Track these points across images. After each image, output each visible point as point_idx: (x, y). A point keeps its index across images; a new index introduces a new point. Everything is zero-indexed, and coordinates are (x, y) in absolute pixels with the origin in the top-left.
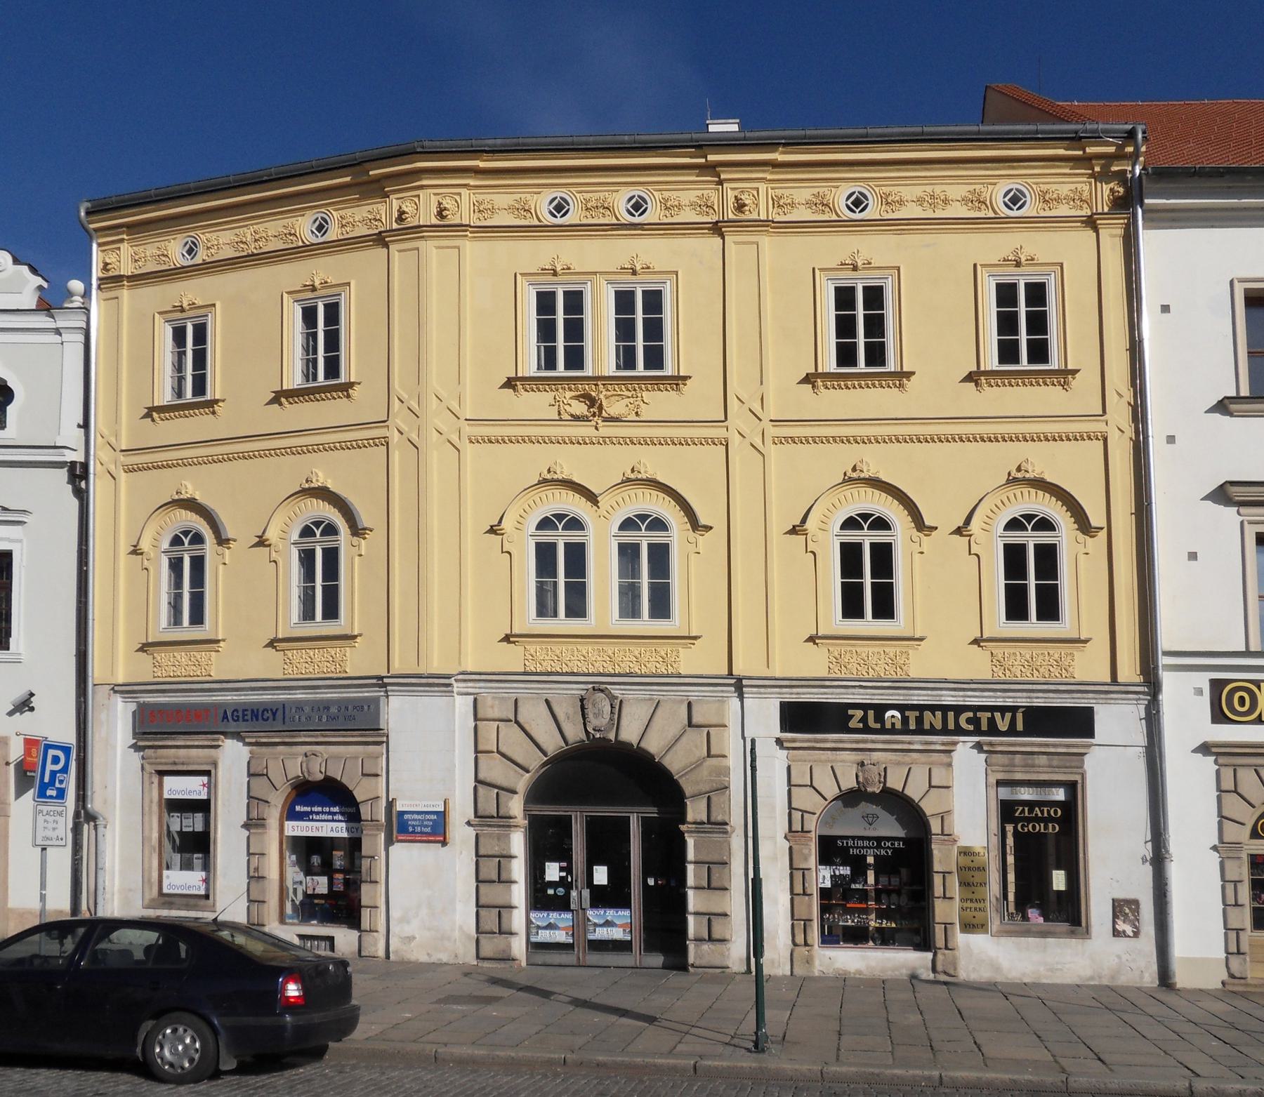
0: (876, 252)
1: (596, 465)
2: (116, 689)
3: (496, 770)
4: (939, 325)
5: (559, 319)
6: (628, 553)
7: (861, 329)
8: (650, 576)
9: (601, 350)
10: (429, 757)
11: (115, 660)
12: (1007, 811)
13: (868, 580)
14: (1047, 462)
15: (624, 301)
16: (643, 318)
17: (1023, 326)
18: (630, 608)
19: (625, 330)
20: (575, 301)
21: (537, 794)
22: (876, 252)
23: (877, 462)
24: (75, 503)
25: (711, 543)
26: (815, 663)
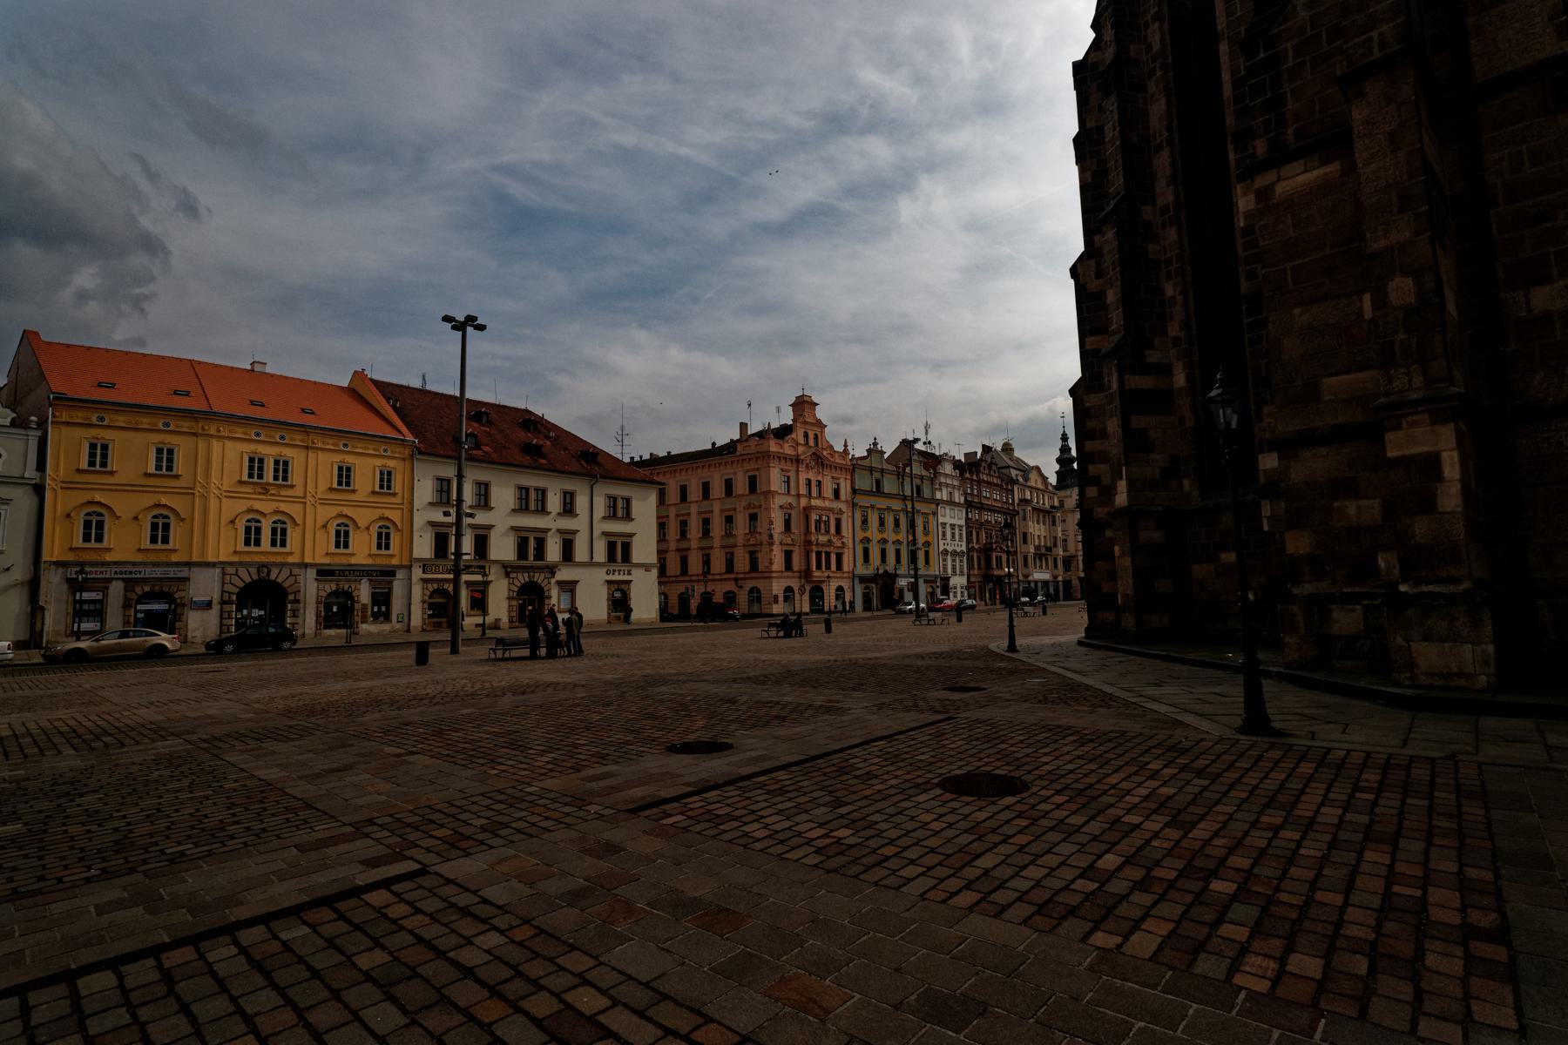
0: (350, 459)
2: (58, 564)
3: (229, 588)
4: (365, 479)
5: (256, 465)
6: (274, 531)
8: (279, 537)
9: (269, 475)
10: (205, 586)
12: (373, 595)
13: (342, 539)
14: (388, 514)
15: (277, 462)
16: (282, 468)
17: (386, 479)
18: (274, 544)
19: (276, 470)
20: (261, 461)
21: (238, 595)
22: (350, 459)
23: (346, 511)
24: (35, 499)
25: (298, 530)
26: (327, 560)
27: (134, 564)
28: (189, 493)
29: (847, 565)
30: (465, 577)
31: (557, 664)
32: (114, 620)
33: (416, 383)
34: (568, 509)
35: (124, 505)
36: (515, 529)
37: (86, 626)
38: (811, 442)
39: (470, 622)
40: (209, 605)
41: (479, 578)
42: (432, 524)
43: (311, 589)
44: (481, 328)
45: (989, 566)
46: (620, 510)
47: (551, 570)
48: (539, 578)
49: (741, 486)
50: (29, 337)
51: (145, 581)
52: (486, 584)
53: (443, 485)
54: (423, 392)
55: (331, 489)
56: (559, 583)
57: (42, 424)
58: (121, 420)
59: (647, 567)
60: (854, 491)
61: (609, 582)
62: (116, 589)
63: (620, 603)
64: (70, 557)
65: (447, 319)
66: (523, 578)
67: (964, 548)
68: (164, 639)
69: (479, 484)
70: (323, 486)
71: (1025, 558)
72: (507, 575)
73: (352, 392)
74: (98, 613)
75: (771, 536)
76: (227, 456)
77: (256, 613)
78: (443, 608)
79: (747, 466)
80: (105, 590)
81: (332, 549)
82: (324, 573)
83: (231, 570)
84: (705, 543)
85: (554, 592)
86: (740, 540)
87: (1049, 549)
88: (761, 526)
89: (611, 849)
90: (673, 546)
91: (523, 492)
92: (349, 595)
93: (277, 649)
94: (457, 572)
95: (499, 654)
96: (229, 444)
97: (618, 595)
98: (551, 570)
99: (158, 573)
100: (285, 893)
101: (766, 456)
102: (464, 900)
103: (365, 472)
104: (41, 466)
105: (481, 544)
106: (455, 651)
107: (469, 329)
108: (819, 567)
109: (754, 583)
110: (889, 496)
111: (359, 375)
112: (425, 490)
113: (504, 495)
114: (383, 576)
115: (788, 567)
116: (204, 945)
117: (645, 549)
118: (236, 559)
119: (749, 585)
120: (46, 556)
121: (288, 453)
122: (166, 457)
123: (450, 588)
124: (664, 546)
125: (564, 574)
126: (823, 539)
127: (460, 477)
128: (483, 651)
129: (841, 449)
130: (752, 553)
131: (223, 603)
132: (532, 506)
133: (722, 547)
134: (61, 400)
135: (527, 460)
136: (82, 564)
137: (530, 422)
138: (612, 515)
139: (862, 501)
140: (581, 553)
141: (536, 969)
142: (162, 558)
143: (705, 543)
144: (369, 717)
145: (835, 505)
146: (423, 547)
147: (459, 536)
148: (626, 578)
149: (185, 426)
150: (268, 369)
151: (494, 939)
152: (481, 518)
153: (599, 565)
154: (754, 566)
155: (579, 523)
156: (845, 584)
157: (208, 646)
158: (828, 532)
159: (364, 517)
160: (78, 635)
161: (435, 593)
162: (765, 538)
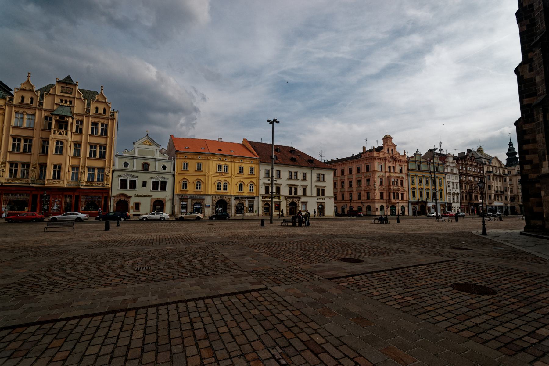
1: (222, 179)
2: (178, 195)
3: (214, 202)
4: (246, 171)
5: (220, 167)
7: (241, 169)
8: (225, 188)
10: (208, 201)
11: (177, 192)
12: (249, 204)
13: (241, 188)
14: (252, 180)
16: (226, 167)
17: (252, 170)
23: (242, 180)
26: (237, 194)
27: (193, 195)
28: (204, 175)
29: (406, 197)
30: (274, 200)
31: (302, 228)
32: (189, 209)
33: (259, 141)
34: (304, 178)
35: (191, 179)
36: (288, 185)
37: (184, 211)
38: (391, 152)
39: (275, 213)
40: (209, 206)
41: (278, 200)
42: (265, 183)
43: (233, 203)
44: (278, 122)
45: (471, 198)
46: (321, 178)
47: (299, 198)
48: (296, 200)
49: (363, 169)
50: (172, 136)
51: (196, 199)
52: (280, 202)
53: (267, 171)
54: (261, 144)
55: (238, 174)
56: (302, 202)
57: (174, 159)
58: (190, 157)
59: (330, 198)
60: (408, 170)
61: (318, 202)
62: (189, 201)
63: (321, 209)
64: (180, 193)
65: (268, 121)
66: (291, 200)
67: (459, 192)
68: (200, 215)
69: (277, 171)
70: (236, 173)
71: (490, 196)
72: (286, 199)
73: (243, 145)
74: (186, 208)
75: (375, 187)
76: (212, 165)
77: (220, 209)
78: (267, 209)
79: (365, 162)
80: (187, 202)
81: (238, 191)
82: (236, 198)
83: (214, 197)
84: (350, 190)
85: (300, 205)
86: (363, 188)
87: (503, 192)
88: (371, 183)
89: (322, 291)
90: (339, 190)
91: (291, 173)
92: (243, 204)
93: (225, 219)
94: (272, 198)
95: (284, 224)
96: (213, 162)
97: (320, 207)
98: (299, 198)
99: (198, 197)
100: (232, 289)
101: (373, 158)
102: (279, 299)
103: (247, 168)
104: (174, 170)
105: (278, 189)
106: (271, 223)
107: (275, 123)
108: (394, 198)
109: (369, 204)
110: (424, 171)
111: (245, 140)
112: (263, 173)
113: (285, 174)
114: (252, 199)
115: (382, 198)
116: (214, 299)
117: (329, 191)
118: (215, 194)
119: (366, 204)
120: (175, 193)
121: (227, 163)
122: (200, 165)
123: (270, 203)
124: (336, 190)
125: (303, 199)
126: (396, 188)
127: (272, 169)
128: (279, 223)
129: (403, 154)
130: (367, 193)
131: (212, 206)
132: (293, 178)
133: (356, 191)
134: (178, 152)
135: (292, 163)
136: (182, 195)
137: (292, 151)
138: (319, 180)
139: (411, 173)
140: (308, 193)
141: (301, 325)
142: (199, 193)
143: (350, 190)
144: (249, 241)
145: (401, 175)
146: (262, 191)
147: (272, 187)
148: (323, 201)
149: (204, 157)
150: (223, 140)
151: (288, 313)
152: (279, 181)
153: (314, 196)
154: (368, 198)
155: (308, 183)
156: (405, 205)
157: (209, 218)
158: (397, 185)
159: (246, 181)
160: (182, 213)
161: (266, 204)
162: (373, 188)
